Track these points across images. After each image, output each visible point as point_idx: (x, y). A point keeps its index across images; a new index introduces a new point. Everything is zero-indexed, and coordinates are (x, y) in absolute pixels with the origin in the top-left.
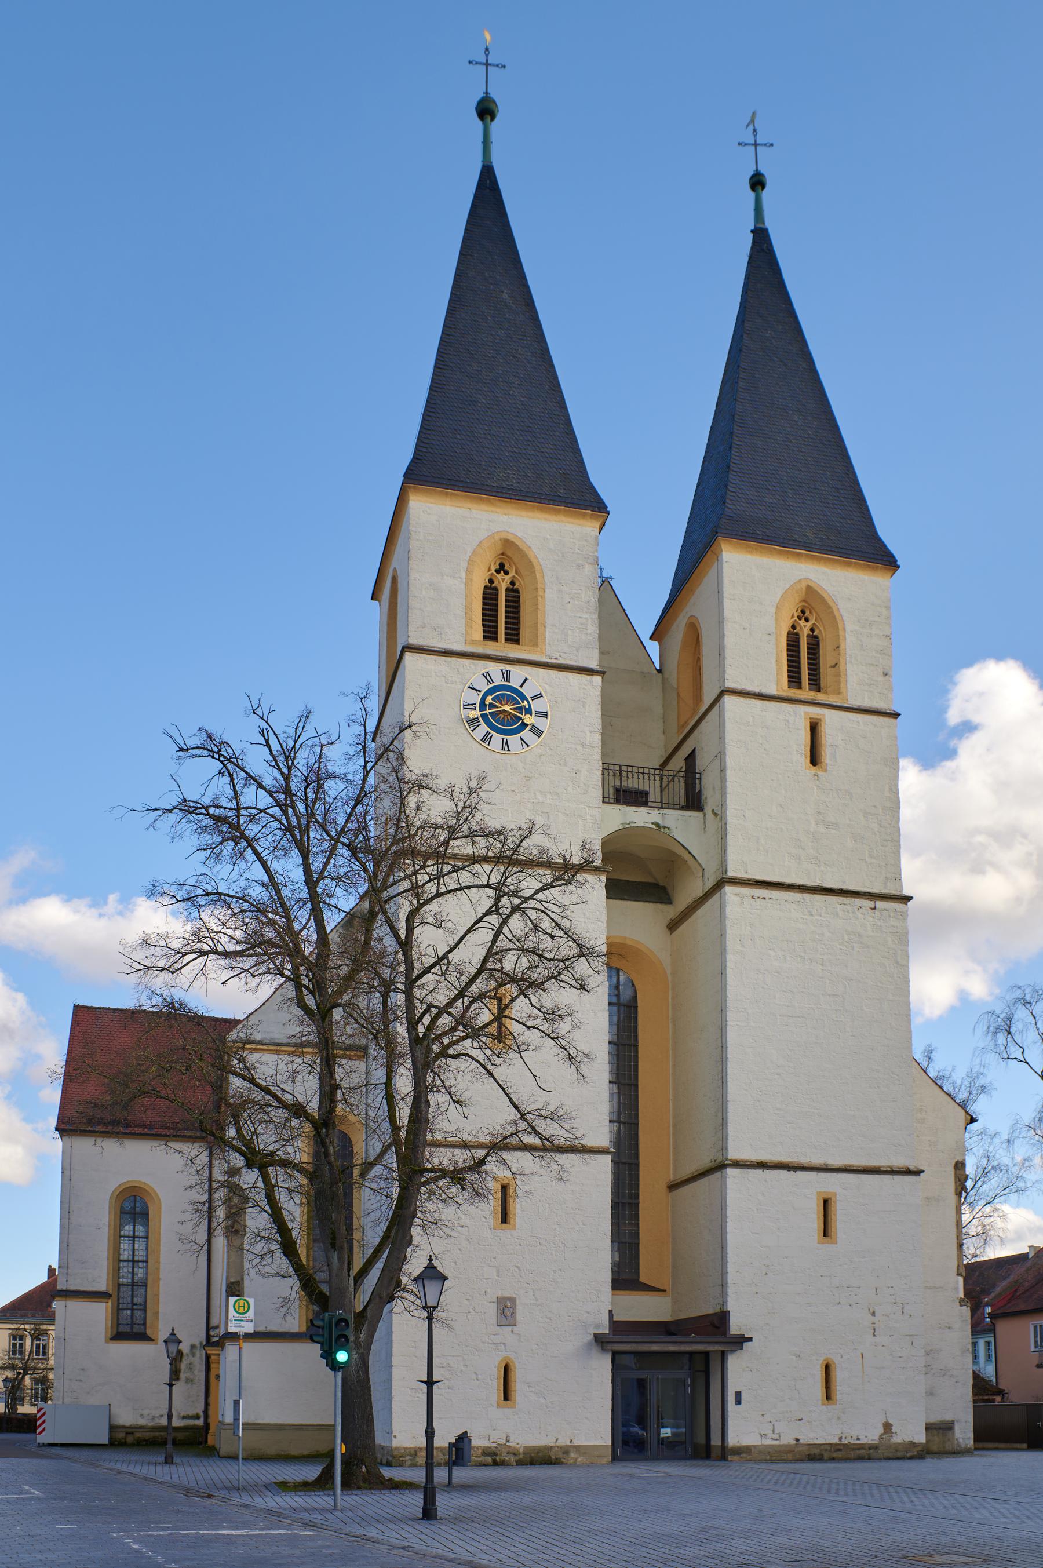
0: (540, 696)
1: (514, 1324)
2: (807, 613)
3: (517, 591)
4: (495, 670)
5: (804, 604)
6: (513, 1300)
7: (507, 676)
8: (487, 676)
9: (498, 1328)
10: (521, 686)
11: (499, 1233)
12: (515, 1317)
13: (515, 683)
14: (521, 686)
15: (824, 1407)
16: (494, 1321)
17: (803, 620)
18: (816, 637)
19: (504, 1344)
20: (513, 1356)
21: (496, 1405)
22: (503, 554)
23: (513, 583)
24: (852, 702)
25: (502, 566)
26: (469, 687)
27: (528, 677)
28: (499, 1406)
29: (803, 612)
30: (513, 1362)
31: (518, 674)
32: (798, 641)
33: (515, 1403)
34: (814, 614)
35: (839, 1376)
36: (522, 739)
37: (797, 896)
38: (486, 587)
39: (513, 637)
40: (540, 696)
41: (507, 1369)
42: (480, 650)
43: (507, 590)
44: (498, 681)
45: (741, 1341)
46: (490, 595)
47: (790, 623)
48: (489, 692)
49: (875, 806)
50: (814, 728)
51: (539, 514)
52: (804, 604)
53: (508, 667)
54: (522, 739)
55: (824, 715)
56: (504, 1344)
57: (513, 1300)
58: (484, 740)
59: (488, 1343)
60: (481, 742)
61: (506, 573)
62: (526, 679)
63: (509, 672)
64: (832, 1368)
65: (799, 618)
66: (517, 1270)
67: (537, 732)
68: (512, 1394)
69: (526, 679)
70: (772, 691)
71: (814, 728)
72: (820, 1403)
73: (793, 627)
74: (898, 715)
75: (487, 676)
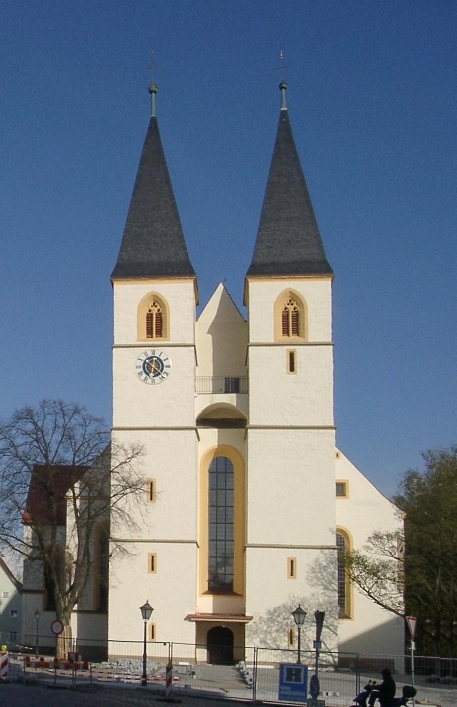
0: (167, 359)
7: (154, 352)
8: (145, 353)
11: (150, 574)
13: (157, 355)
20: (155, 622)
29: (290, 301)
30: (155, 624)
32: (288, 315)
37: (282, 431)
39: (159, 333)
40: (167, 359)
41: (153, 627)
44: (150, 355)
47: (283, 307)
50: (292, 356)
53: (154, 348)
55: (296, 349)
58: (144, 380)
63: (154, 351)
68: (154, 637)
70: (272, 341)
71: (292, 356)
75: (145, 353)
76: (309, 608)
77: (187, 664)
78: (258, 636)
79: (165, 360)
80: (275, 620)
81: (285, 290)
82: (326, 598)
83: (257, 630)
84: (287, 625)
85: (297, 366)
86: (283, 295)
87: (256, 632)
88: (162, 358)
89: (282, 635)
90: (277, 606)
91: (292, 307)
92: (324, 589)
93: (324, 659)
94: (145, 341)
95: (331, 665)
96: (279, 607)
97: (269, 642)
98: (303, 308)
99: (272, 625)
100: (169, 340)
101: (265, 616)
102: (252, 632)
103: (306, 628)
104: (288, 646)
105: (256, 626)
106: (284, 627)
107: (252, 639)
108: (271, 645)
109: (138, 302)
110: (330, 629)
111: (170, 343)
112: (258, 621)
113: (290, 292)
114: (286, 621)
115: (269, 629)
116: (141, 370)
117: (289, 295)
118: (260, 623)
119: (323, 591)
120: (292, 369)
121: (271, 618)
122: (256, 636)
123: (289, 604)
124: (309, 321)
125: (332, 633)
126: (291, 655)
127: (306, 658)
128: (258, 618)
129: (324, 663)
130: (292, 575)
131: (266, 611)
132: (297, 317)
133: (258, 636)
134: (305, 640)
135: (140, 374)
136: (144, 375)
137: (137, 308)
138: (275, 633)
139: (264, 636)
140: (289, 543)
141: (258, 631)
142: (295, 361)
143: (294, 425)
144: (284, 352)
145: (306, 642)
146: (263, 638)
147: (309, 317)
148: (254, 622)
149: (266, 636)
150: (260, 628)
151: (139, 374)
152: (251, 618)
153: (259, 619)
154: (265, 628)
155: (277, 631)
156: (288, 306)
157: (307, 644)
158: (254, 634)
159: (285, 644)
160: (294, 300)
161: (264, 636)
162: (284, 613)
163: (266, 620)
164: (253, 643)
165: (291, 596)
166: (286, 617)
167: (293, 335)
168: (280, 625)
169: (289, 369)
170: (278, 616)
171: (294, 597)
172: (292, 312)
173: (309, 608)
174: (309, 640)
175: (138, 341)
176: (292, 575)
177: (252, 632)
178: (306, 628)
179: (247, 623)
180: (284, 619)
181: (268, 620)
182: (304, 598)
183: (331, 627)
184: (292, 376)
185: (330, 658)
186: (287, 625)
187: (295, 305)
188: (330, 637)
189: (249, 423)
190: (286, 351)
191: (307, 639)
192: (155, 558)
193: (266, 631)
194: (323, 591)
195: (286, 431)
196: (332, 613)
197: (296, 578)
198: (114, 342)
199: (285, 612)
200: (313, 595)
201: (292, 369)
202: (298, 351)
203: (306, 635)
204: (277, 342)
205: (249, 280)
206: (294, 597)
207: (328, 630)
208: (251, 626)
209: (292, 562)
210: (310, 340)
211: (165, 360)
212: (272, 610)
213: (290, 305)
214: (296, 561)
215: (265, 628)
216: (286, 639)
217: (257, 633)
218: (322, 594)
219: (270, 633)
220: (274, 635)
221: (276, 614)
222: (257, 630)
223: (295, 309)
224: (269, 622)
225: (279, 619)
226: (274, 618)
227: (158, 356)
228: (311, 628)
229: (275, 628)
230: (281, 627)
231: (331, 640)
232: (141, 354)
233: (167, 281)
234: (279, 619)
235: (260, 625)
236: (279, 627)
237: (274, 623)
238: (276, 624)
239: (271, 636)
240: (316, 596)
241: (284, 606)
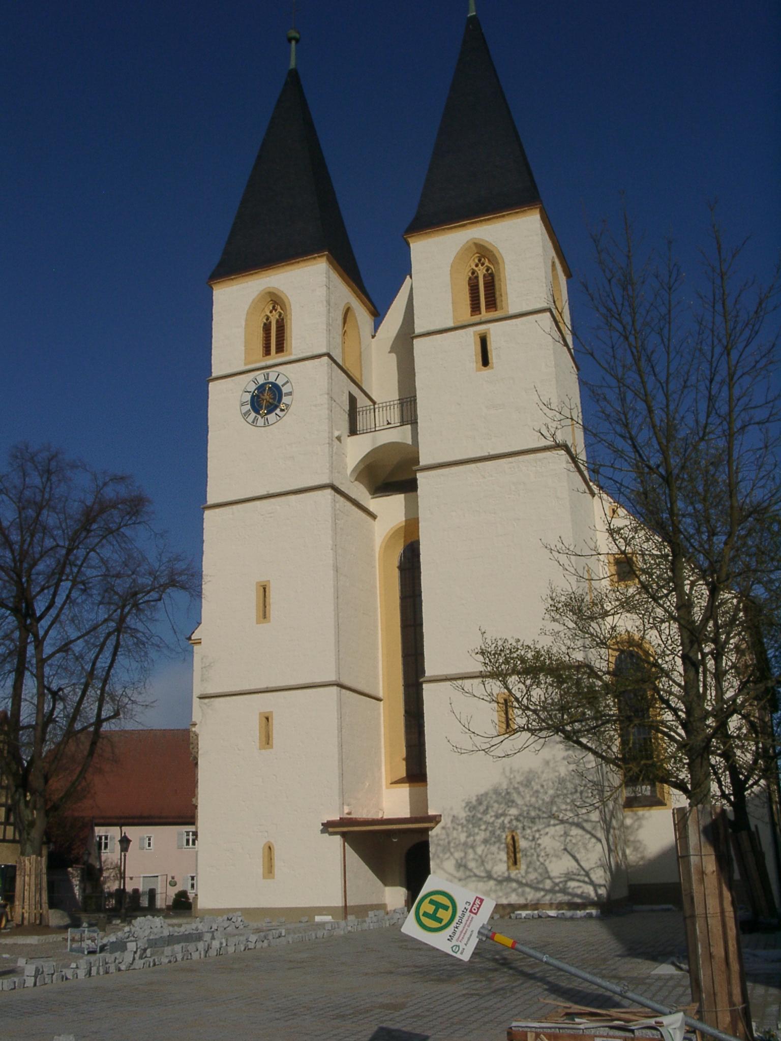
17: (480, 266)
20: (272, 841)
39: (280, 348)
42: (263, 364)
44: (261, 381)
46: (267, 328)
47: (468, 269)
50: (483, 342)
53: (268, 370)
58: (253, 422)
63: (268, 374)
70: (451, 324)
71: (483, 342)
76: (542, 791)
77: (328, 918)
78: (452, 854)
79: (283, 386)
80: (481, 819)
81: (467, 242)
82: (573, 767)
83: (449, 843)
84: (503, 827)
86: (466, 250)
87: (446, 849)
88: (280, 382)
89: (494, 849)
90: (482, 791)
92: (567, 750)
93: (579, 891)
95: (593, 904)
96: (486, 794)
97: (472, 865)
98: (498, 263)
99: (476, 830)
101: (463, 815)
102: (440, 848)
103: (538, 831)
104: (508, 869)
105: (448, 835)
106: (498, 832)
107: (442, 861)
108: (475, 871)
109: (247, 307)
110: (583, 828)
111: (293, 357)
112: (449, 825)
113: (476, 245)
114: (500, 821)
115: (472, 838)
116: (249, 407)
117: (474, 250)
118: (454, 828)
119: (566, 754)
120: (485, 362)
121: (473, 817)
122: (448, 855)
123: (505, 786)
124: (508, 282)
125: (588, 836)
126: (515, 890)
127: (542, 893)
128: (449, 820)
129: (578, 900)
131: (464, 805)
132: (491, 284)
133: (452, 854)
134: (538, 856)
135: (246, 415)
136: (253, 414)
138: (483, 847)
139: (462, 854)
141: (452, 845)
143: (492, 453)
144: (469, 337)
145: (541, 859)
146: (461, 859)
147: (508, 277)
148: (443, 828)
149: (466, 853)
150: (455, 839)
151: (245, 414)
152: (436, 819)
153: (452, 821)
154: (463, 837)
155: (485, 841)
156: (476, 269)
157: (542, 864)
158: (444, 852)
159: (501, 868)
160: (484, 257)
161: (462, 854)
162: (496, 805)
163: (465, 823)
164: (443, 869)
165: (507, 769)
166: (500, 811)
168: (490, 829)
169: (481, 363)
170: (485, 812)
171: (511, 771)
173: (542, 791)
174: (547, 855)
175: (246, 364)
177: (440, 848)
178: (538, 831)
179: (432, 828)
180: (497, 817)
181: (468, 821)
182: (530, 771)
183: (585, 825)
184: (486, 372)
185: (590, 890)
186: (503, 827)
187: (487, 263)
188: (585, 847)
190: (472, 333)
191: (543, 854)
193: (465, 844)
194: (566, 754)
195: (479, 465)
196: (585, 794)
198: (211, 373)
199: (497, 801)
200: (547, 763)
201: (485, 362)
203: (539, 845)
204: (459, 324)
205: (410, 240)
206: (511, 771)
207: (580, 832)
208: (437, 835)
210: (512, 310)
212: (474, 800)
215: (463, 837)
216: (503, 856)
217: (449, 850)
218: (564, 758)
219: (473, 847)
220: (479, 850)
221: (482, 808)
222: (449, 843)
223: (487, 270)
224: (470, 826)
225: (489, 818)
226: (479, 816)
227: (273, 381)
228: (547, 830)
229: (481, 836)
230: (493, 833)
231: (587, 850)
232: (248, 384)
233: (288, 268)
234: (489, 818)
235: (455, 834)
236: (488, 833)
237: (479, 826)
238: (483, 827)
239: (475, 853)
240: (551, 765)
241: (496, 792)
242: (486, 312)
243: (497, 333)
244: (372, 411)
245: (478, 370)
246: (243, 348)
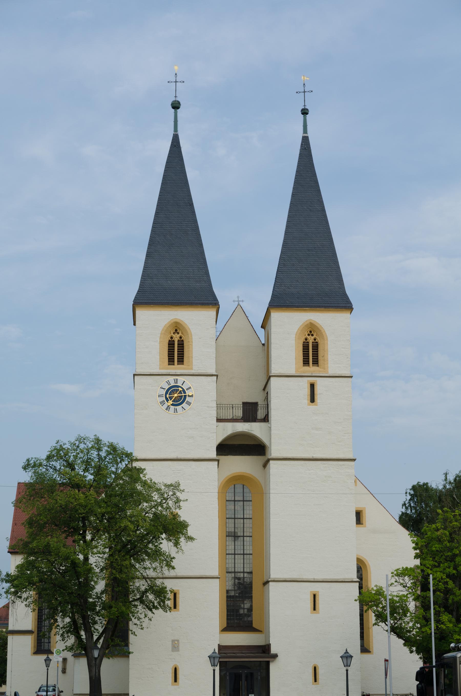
0: (190, 388)
1: (178, 651)
2: (312, 333)
3: (183, 341)
4: (171, 379)
5: (310, 329)
6: (178, 641)
7: (176, 381)
8: (168, 382)
9: (172, 652)
10: (182, 385)
12: (179, 648)
14: (182, 385)
15: (313, 685)
16: (170, 649)
18: (317, 342)
19: (174, 659)
21: (171, 684)
22: (176, 326)
23: (181, 337)
24: (331, 373)
25: (176, 330)
26: (161, 388)
27: (185, 380)
28: (172, 685)
29: (311, 332)
31: (181, 379)
33: (179, 683)
34: (315, 333)
35: (320, 672)
36: (182, 407)
38: (169, 341)
39: (181, 361)
40: (190, 388)
43: (178, 341)
44: (173, 384)
45: (275, 656)
46: (171, 344)
47: (304, 337)
48: (166, 393)
49: (340, 419)
50: (312, 386)
51: (190, 309)
52: (310, 329)
54: (182, 407)
56: (174, 659)
57: (178, 641)
58: (166, 409)
59: (168, 659)
60: (166, 410)
61: (178, 333)
62: (184, 381)
63: (177, 379)
64: (317, 668)
65: (309, 335)
66: (179, 628)
67: (189, 403)
69: (184, 381)
70: (293, 372)
71: (312, 386)
72: (311, 683)
73: (306, 339)
74: (352, 376)
75: (168, 382)
79: (187, 389)
85: (318, 397)
91: (313, 338)
94: (167, 369)
100: (192, 369)
113: (311, 323)
120: (312, 400)
130: (314, 609)
137: (159, 335)
140: (311, 577)
142: (315, 392)
144: (304, 384)
151: (161, 403)
167: (313, 366)
172: (313, 342)
175: (160, 369)
176: (314, 609)
184: (312, 407)
189: (271, 454)
190: (307, 381)
192: (177, 595)
197: (319, 613)
201: (312, 400)
202: (318, 383)
209: (315, 596)
210: (331, 372)
211: (187, 389)
213: (310, 336)
214: (318, 595)
242: (313, 366)
243: (320, 384)
244: (231, 408)
245: (309, 405)
246: (159, 357)
